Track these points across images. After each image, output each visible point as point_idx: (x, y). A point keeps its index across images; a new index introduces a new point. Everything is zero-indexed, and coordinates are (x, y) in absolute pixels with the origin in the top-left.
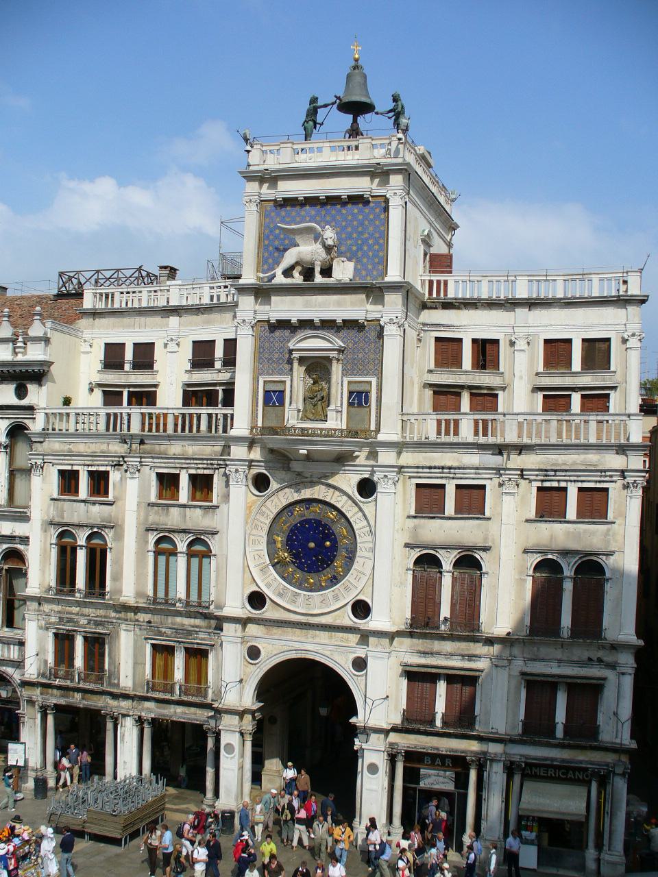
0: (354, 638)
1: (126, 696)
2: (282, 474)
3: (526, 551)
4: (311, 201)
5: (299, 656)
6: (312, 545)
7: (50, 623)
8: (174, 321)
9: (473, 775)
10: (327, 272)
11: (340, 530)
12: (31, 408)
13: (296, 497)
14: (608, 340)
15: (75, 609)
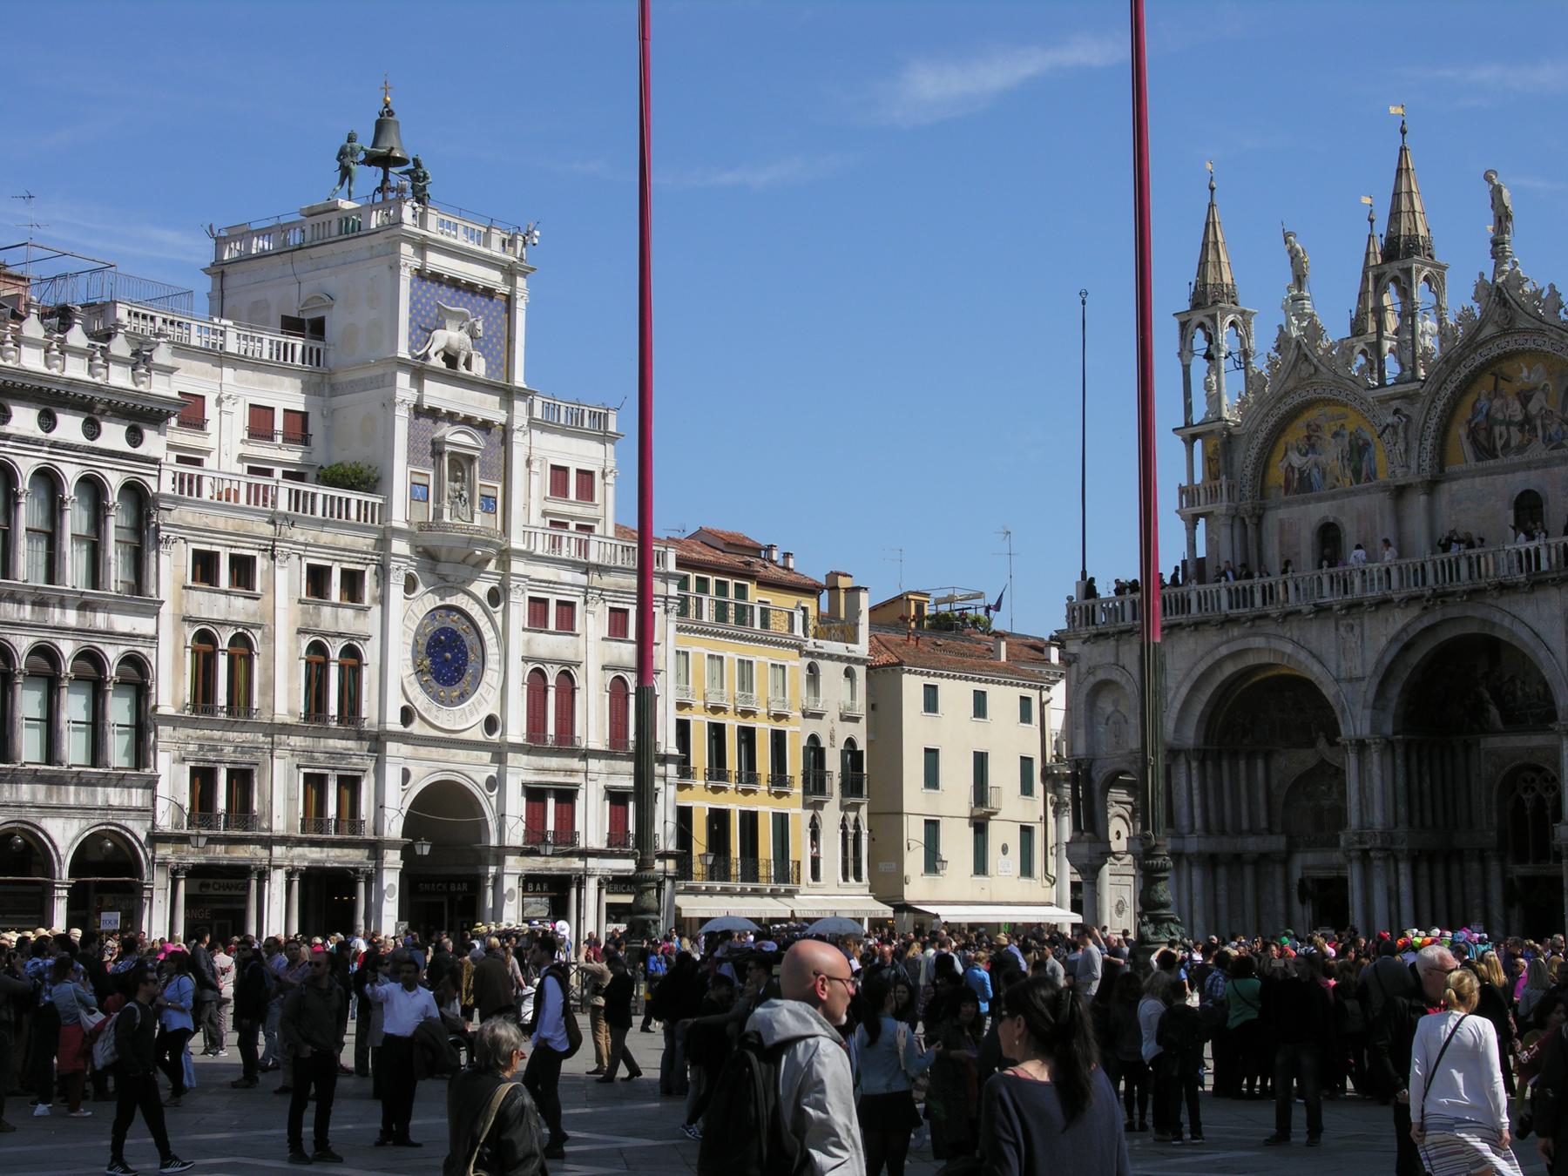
0: (487, 756)
1: (284, 841)
2: (427, 576)
3: (604, 668)
4: (454, 283)
5: (444, 778)
6: (448, 655)
7: (191, 753)
8: (228, 372)
9: (574, 891)
10: (468, 364)
11: (470, 640)
12: (156, 461)
13: (440, 603)
14: (591, 474)
15: (217, 734)
